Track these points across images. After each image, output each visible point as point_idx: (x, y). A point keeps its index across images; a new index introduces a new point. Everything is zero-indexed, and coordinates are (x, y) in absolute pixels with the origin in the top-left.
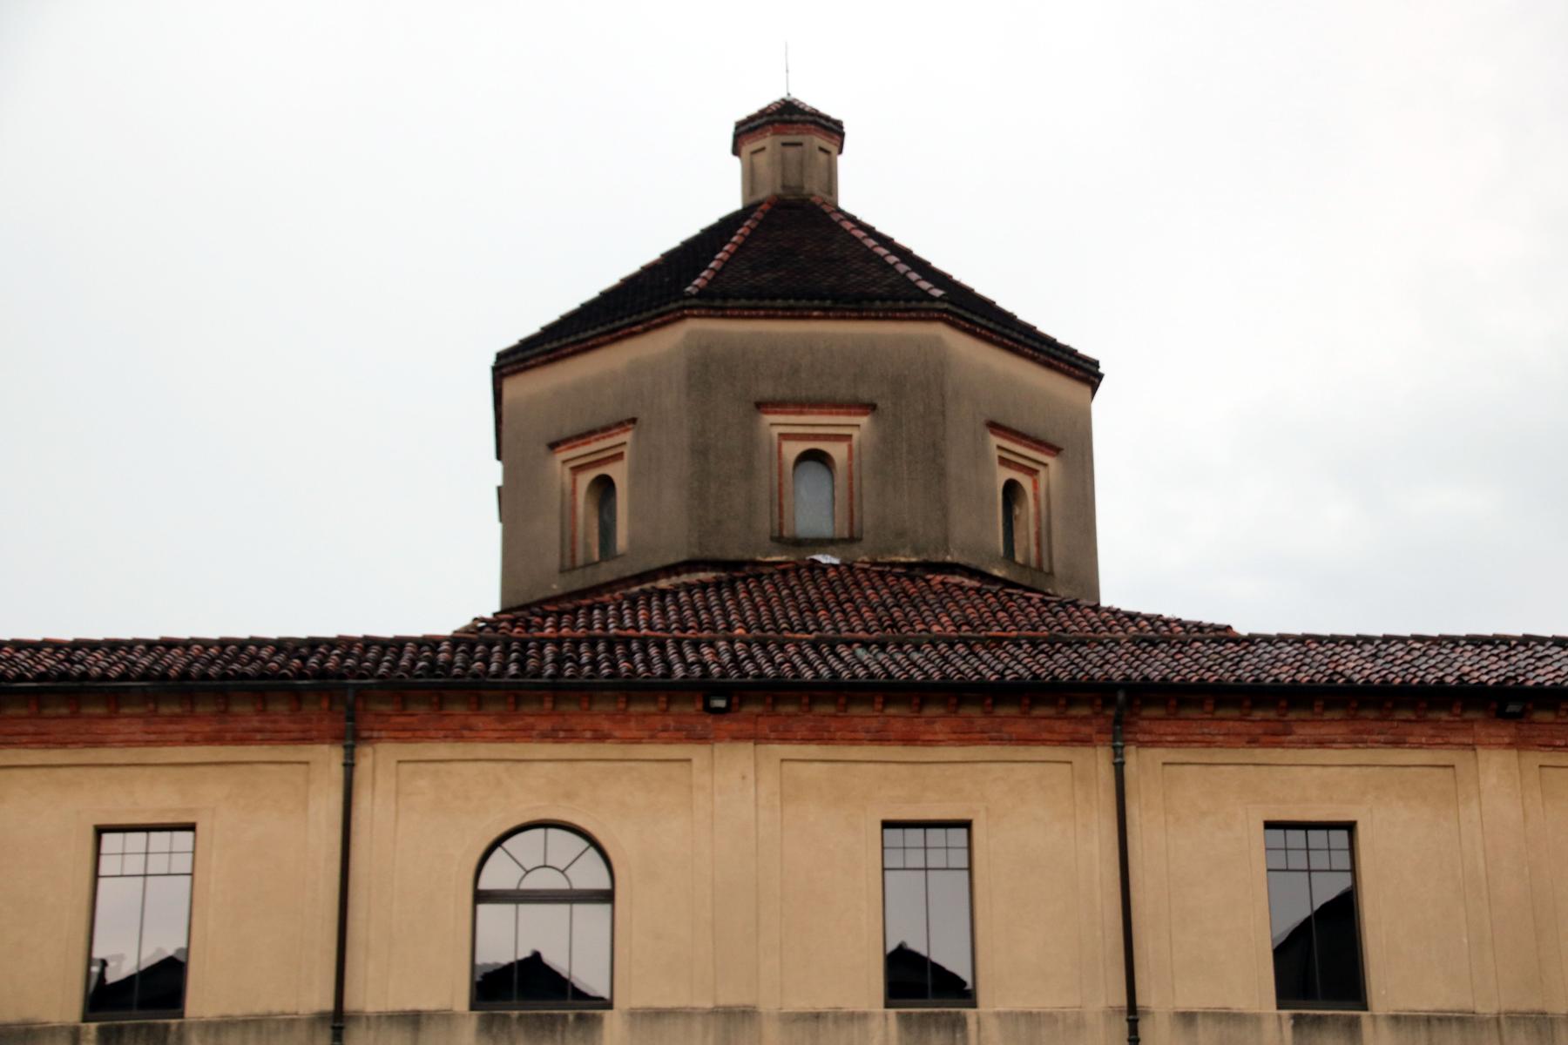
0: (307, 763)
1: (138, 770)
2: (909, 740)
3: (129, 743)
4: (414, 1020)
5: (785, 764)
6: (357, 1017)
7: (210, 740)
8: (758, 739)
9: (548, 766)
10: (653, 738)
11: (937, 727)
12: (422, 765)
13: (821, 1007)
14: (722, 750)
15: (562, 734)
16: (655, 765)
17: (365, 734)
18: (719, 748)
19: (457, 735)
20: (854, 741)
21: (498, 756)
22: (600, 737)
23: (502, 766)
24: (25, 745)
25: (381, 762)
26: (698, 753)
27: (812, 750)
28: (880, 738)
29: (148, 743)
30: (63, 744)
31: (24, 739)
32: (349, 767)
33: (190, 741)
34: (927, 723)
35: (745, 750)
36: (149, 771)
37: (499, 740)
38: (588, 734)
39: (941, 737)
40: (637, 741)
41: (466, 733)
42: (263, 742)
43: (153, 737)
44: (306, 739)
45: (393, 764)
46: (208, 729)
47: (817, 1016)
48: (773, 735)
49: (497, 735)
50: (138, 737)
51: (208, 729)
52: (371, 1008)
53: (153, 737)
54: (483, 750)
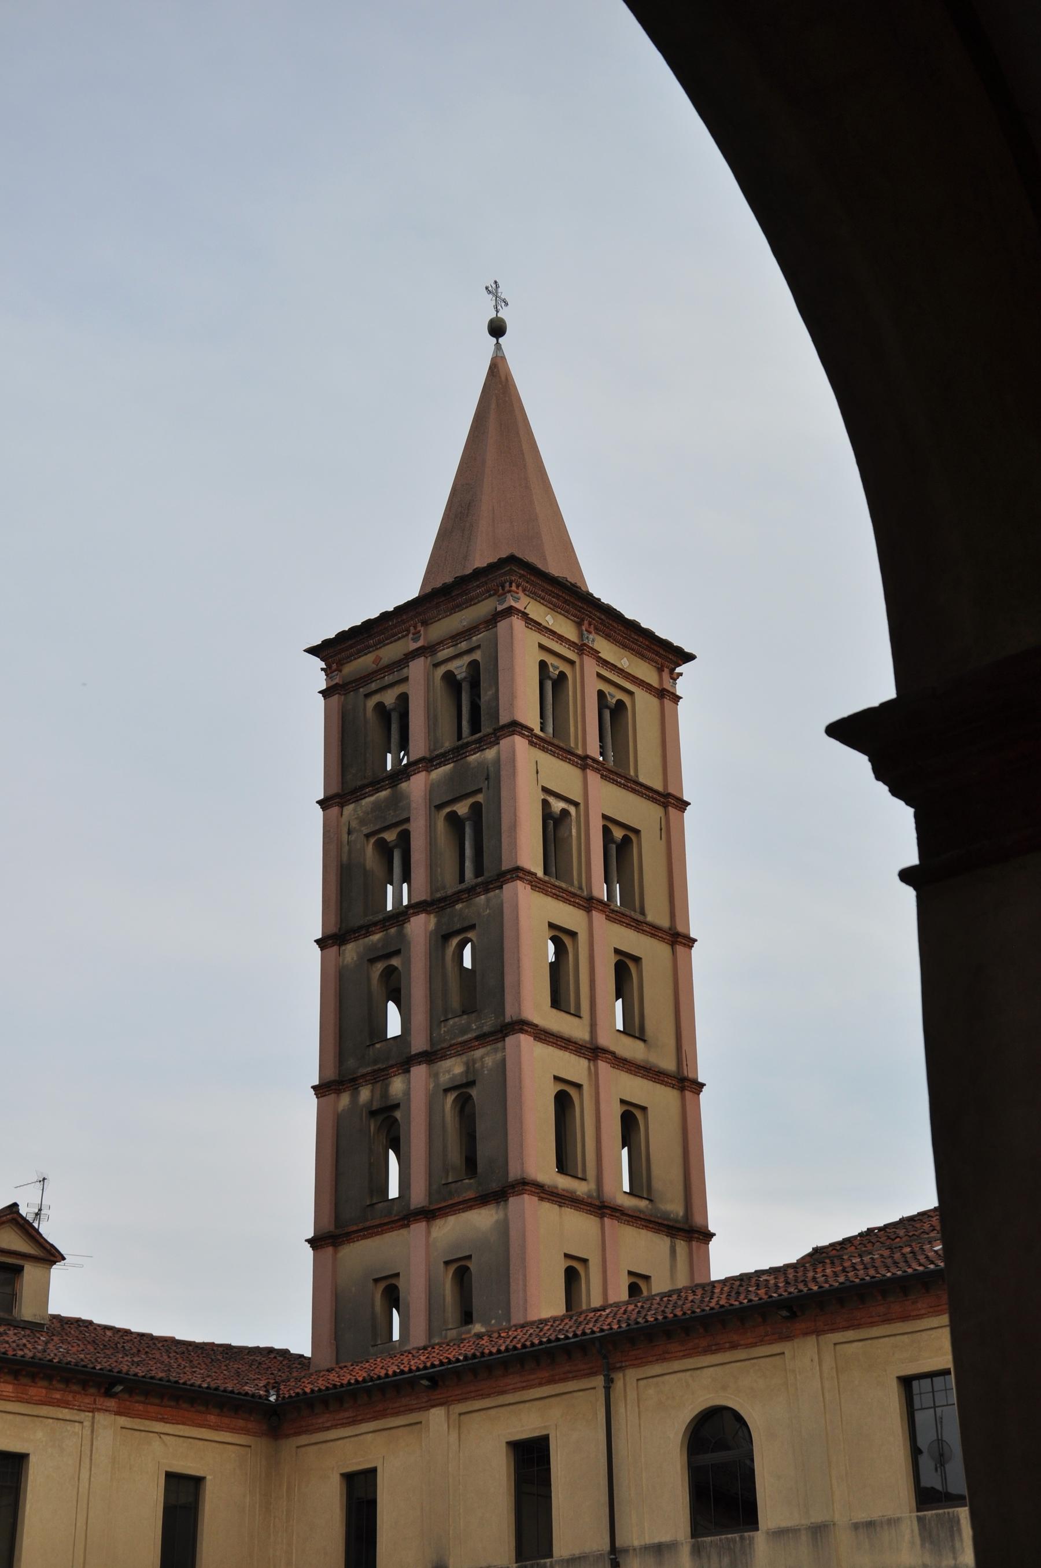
0: (594, 1388)
1: (522, 1406)
2: (905, 1318)
3: (515, 1390)
4: (659, 1550)
5: (838, 1347)
6: (625, 1551)
7: (551, 1381)
8: (818, 1332)
9: (711, 1369)
10: (761, 1342)
11: (919, 1305)
12: (650, 1380)
13: (875, 1515)
14: (797, 1343)
15: (714, 1348)
16: (768, 1359)
17: (618, 1365)
18: (796, 1340)
19: (662, 1358)
20: (872, 1324)
21: (684, 1368)
22: (734, 1346)
23: (688, 1373)
24: (473, 1398)
25: (627, 1381)
26: (785, 1347)
27: (850, 1334)
28: (887, 1320)
29: (523, 1388)
30: (488, 1395)
31: (473, 1394)
32: (608, 1389)
33: (541, 1385)
34: (913, 1303)
35: (811, 1341)
36: (527, 1405)
37: (685, 1357)
38: (727, 1345)
39: (923, 1312)
40: (754, 1345)
41: (667, 1356)
42: (574, 1378)
43: (525, 1384)
44: (593, 1374)
45: (635, 1384)
46: (547, 1375)
47: (870, 1524)
48: (826, 1328)
49: (681, 1354)
50: (519, 1385)
51: (547, 1375)
52: (636, 1543)
53: (525, 1384)
54: (676, 1365)
